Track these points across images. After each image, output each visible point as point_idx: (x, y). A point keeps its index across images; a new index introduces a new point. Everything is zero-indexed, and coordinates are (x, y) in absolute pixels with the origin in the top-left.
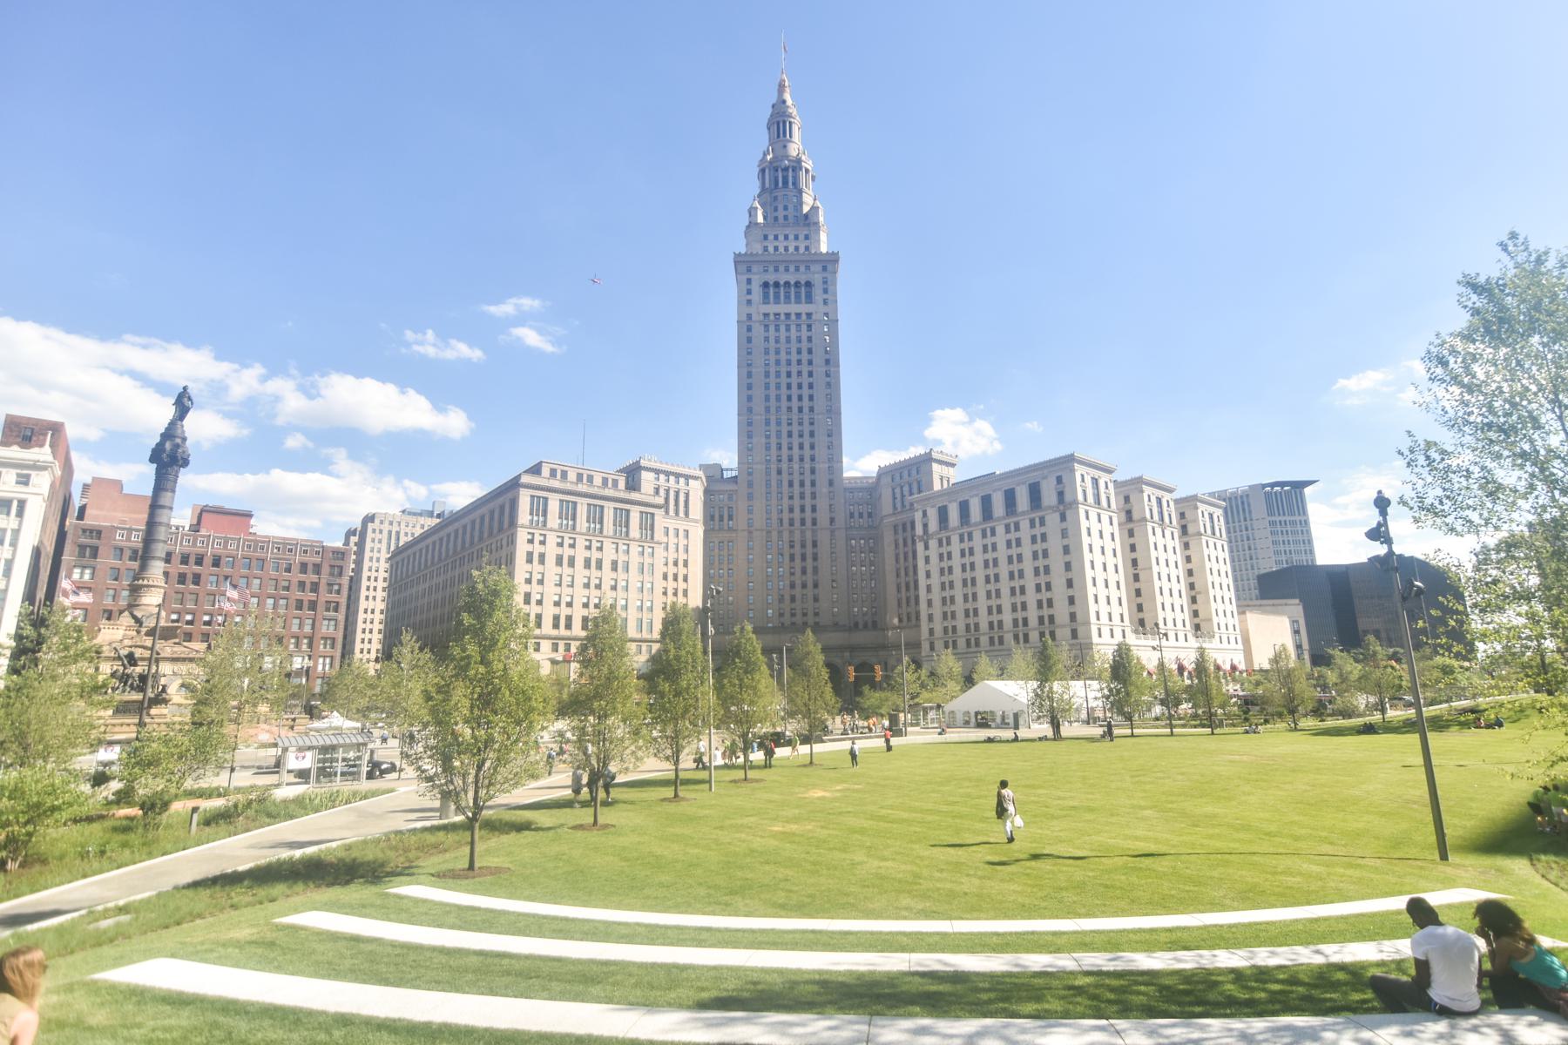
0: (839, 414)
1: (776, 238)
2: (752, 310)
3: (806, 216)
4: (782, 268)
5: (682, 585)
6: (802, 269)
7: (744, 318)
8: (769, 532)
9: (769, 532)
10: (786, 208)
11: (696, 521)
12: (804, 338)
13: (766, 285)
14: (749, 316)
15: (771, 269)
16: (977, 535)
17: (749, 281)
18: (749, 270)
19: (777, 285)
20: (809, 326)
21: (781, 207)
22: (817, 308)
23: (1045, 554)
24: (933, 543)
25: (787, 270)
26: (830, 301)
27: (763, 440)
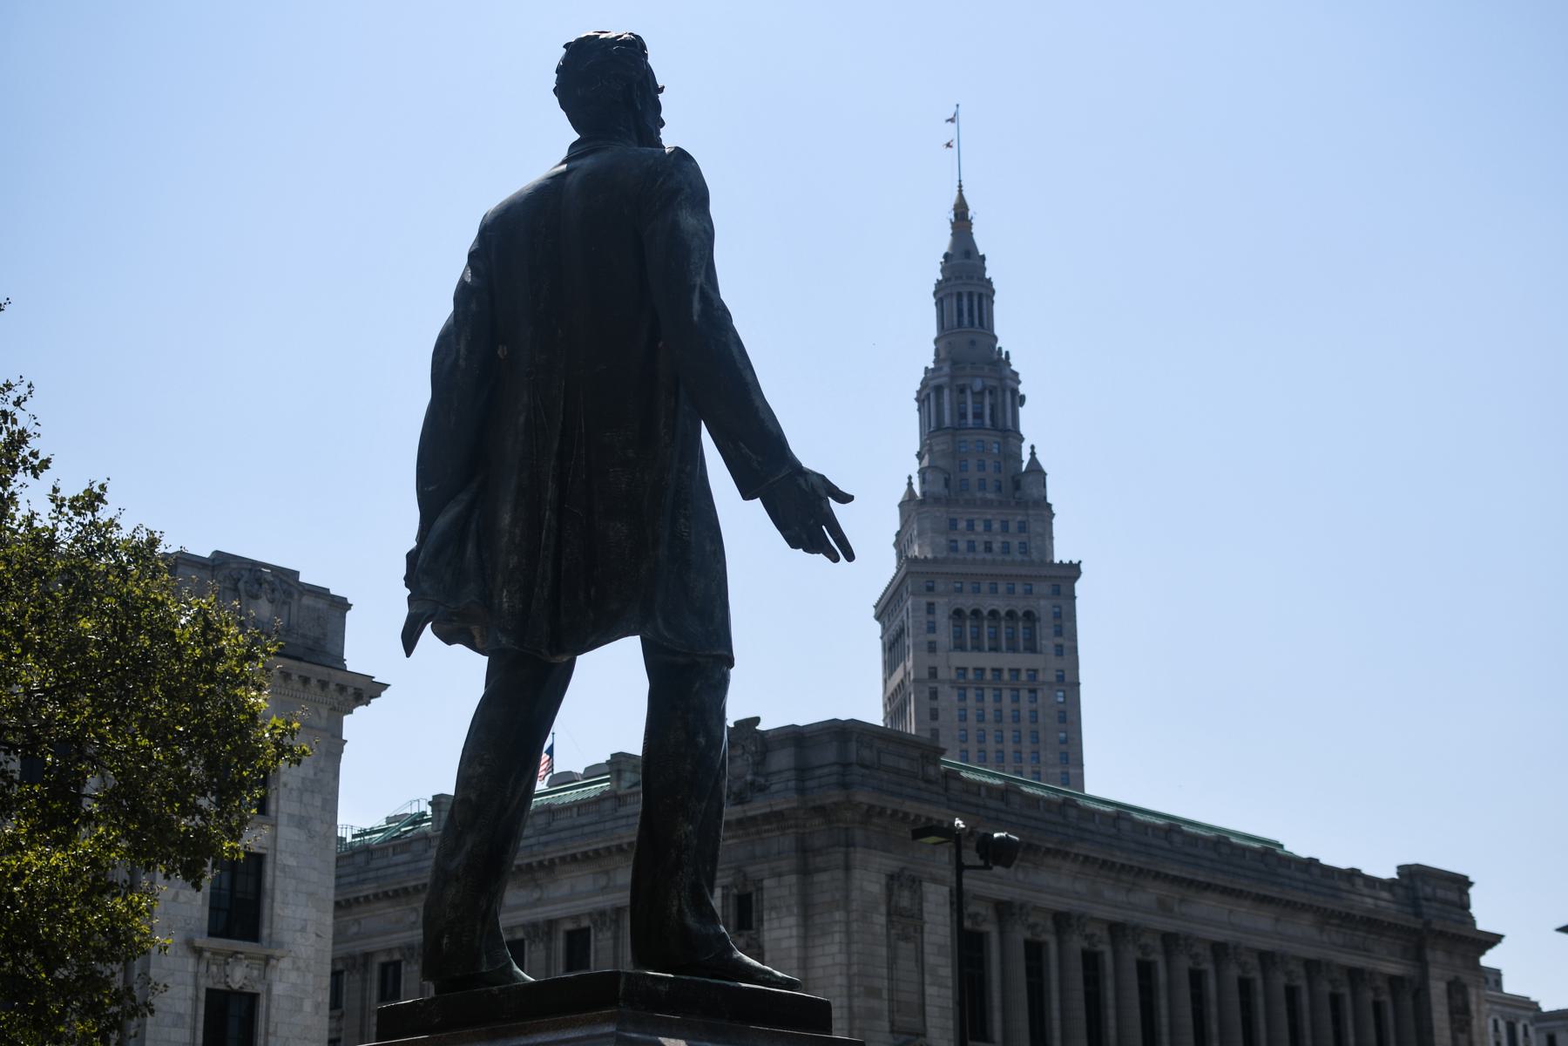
1: (971, 525)
2: (939, 660)
4: (985, 587)
7: (925, 674)
10: (982, 467)
12: (1025, 714)
13: (958, 614)
14: (933, 673)
17: (931, 608)
18: (930, 589)
19: (976, 613)
20: (1033, 691)
21: (972, 463)
25: (994, 590)
26: (1067, 649)
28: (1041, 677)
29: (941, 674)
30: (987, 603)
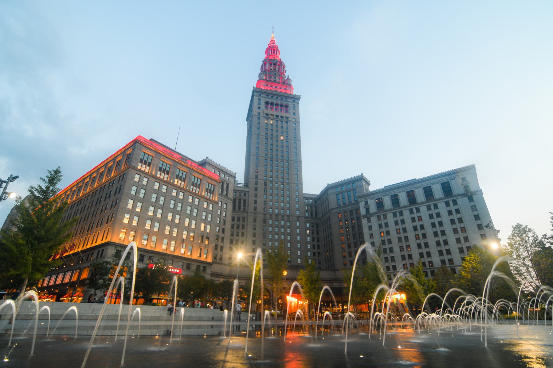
0: (301, 162)
1: (272, 86)
3: (284, 82)
4: (275, 97)
5: (221, 234)
6: (284, 99)
7: (257, 114)
8: (265, 214)
9: (265, 214)
10: (275, 77)
11: (230, 199)
13: (267, 103)
15: (270, 97)
16: (406, 213)
17: (260, 99)
19: (272, 104)
20: (287, 122)
21: (273, 77)
22: (290, 115)
23: (460, 220)
24: (374, 219)
26: (296, 113)
27: (263, 169)
28: (289, 119)
29: (262, 114)
30: (275, 102)
